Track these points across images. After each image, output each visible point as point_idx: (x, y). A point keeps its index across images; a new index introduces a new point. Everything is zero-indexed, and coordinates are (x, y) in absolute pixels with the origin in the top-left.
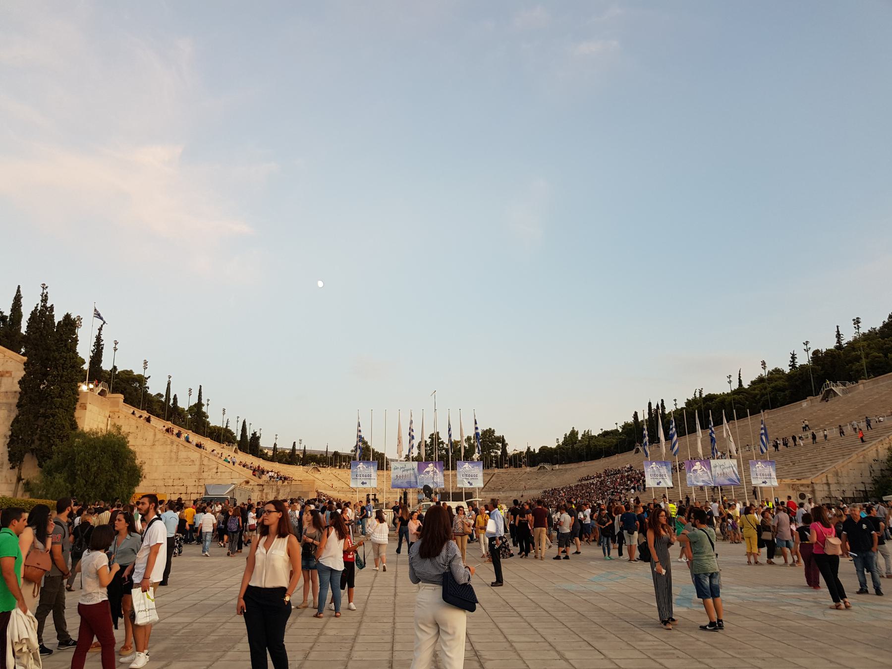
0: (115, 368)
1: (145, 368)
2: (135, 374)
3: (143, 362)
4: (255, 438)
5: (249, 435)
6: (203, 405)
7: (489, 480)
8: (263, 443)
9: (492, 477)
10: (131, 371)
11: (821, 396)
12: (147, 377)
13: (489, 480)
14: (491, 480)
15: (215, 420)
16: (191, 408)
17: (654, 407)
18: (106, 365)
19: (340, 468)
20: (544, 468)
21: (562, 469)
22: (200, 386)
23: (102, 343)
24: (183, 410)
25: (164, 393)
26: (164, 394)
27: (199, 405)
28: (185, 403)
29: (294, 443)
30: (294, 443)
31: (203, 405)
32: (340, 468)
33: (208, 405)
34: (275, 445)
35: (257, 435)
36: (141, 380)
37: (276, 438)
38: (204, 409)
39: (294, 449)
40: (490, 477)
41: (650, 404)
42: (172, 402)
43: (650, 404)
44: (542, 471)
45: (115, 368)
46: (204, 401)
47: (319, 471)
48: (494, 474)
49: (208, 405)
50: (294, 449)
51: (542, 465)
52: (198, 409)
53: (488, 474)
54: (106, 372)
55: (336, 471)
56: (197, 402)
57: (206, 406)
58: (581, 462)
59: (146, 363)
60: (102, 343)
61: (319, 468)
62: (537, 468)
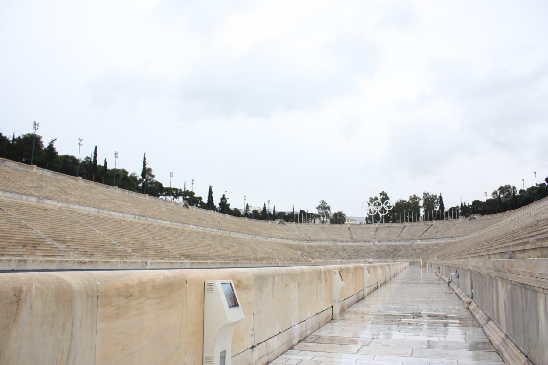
7: (426, 230)
9: (430, 227)
13: (426, 230)
14: (428, 230)
20: (474, 218)
21: (489, 219)
29: (265, 203)
30: (265, 203)
34: (247, 206)
37: (245, 199)
39: (265, 208)
40: (428, 227)
44: (473, 220)
47: (285, 224)
48: (432, 225)
50: (265, 208)
51: (472, 215)
53: (428, 225)
58: (506, 211)
61: (285, 223)
62: (469, 218)
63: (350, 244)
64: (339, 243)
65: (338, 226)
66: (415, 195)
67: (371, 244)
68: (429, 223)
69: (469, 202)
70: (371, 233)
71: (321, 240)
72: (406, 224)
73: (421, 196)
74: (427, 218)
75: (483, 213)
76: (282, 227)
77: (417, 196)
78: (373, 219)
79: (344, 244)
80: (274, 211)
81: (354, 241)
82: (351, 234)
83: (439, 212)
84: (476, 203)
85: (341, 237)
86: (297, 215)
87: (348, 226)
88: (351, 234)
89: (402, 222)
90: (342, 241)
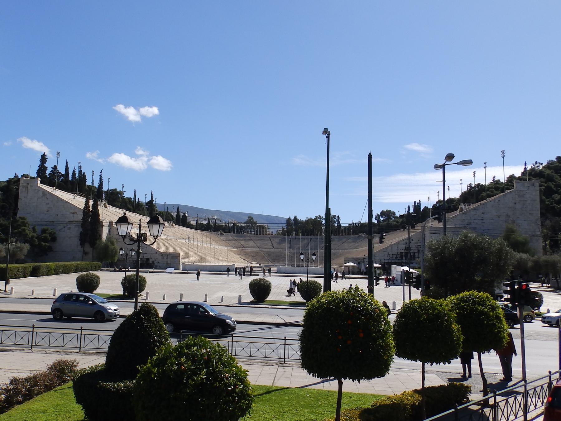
0: (109, 189)
2: (118, 190)
4: (185, 217)
6: (154, 201)
10: (116, 189)
12: (124, 191)
17: (416, 204)
18: (105, 189)
19: (237, 233)
22: (152, 191)
23: (102, 179)
25: (133, 197)
27: (152, 201)
31: (154, 201)
32: (237, 233)
33: (156, 201)
36: (121, 193)
41: (415, 201)
43: (415, 201)
45: (109, 189)
49: (156, 201)
56: (150, 199)
60: (102, 179)
82: (272, 243)
85: (265, 245)
88: (272, 243)
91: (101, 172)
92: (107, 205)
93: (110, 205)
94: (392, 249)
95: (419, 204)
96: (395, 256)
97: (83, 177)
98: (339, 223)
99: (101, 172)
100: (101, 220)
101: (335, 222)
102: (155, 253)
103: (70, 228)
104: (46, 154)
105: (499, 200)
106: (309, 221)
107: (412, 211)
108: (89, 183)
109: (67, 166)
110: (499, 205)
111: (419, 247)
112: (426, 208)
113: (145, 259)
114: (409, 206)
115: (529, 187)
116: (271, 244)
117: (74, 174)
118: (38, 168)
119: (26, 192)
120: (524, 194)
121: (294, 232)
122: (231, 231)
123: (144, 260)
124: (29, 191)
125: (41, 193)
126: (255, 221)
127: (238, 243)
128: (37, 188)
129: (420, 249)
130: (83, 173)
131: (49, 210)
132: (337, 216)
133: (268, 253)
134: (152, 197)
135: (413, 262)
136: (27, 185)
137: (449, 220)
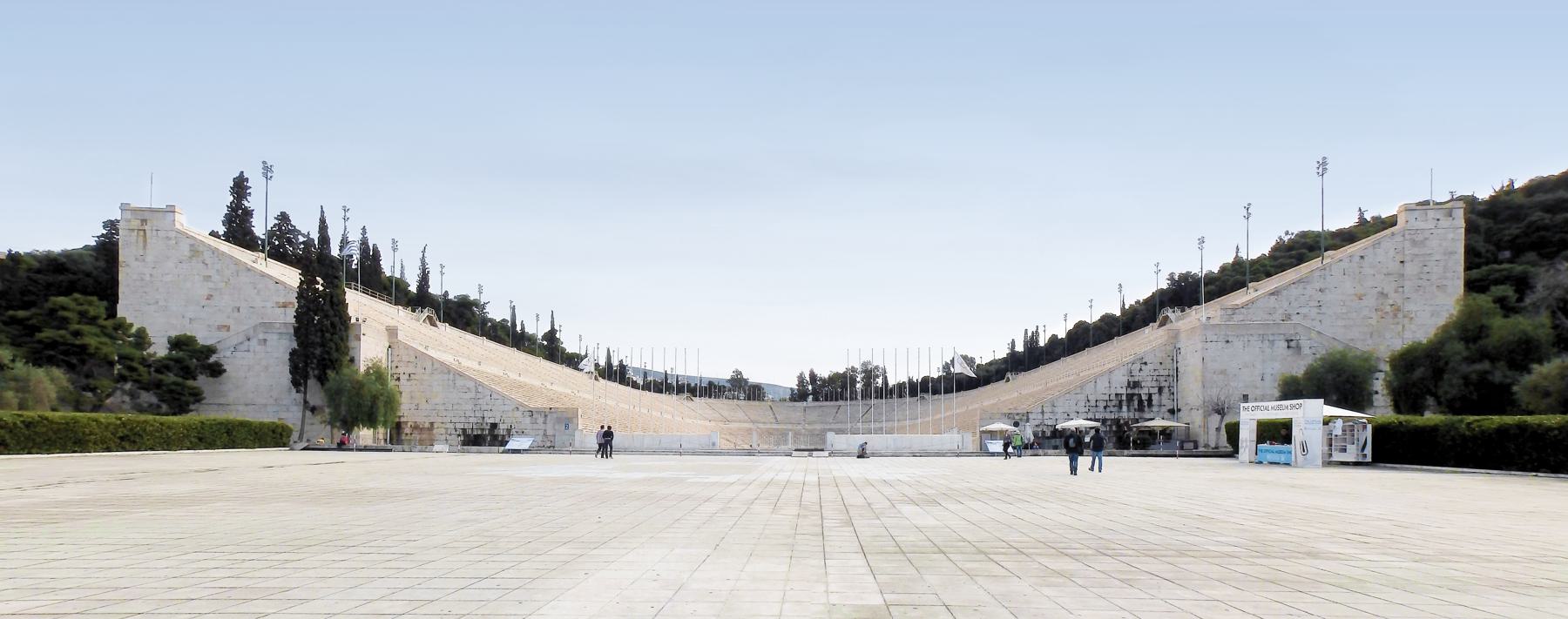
1: (481, 293)
2: (472, 299)
3: (477, 287)
4: (623, 367)
5: (615, 363)
8: (630, 374)
11: (1158, 323)
15: (570, 345)
16: (545, 337)
17: (1030, 334)
24: (533, 335)
26: (509, 320)
28: (538, 329)
35: (624, 363)
38: (558, 336)
42: (519, 328)
46: (557, 327)
52: (551, 336)
54: (435, 296)
55: (712, 401)
57: (558, 333)
59: (480, 287)
61: (693, 398)
63: (775, 426)
64: (761, 426)
65: (757, 403)
66: (852, 367)
67: (799, 427)
68: (868, 402)
69: (917, 377)
70: (798, 414)
71: (740, 421)
72: (840, 403)
73: (858, 366)
74: (866, 394)
75: (936, 392)
76: (690, 404)
77: (856, 367)
78: (799, 395)
79: (768, 426)
80: (677, 381)
81: (777, 422)
83: (882, 388)
84: (925, 380)
86: (705, 387)
87: (770, 403)
89: (836, 400)
90: (764, 423)
91: (424, 252)
92: (438, 323)
93: (447, 324)
94: (1095, 386)
95: (1036, 334)
96: (1102, 404)
97: (371, 258)
98: (885, 379)
99: (424, 252)
100: (353, 321)
101: (878, 376)
102: (513, 410)
103: (265, 340)
104: (246, 176)
105: (1362, 257)
106: (834, 378)
107: (1020, 348)
108: (387, 267)
109: (323, 222)
110: (1361, 267)
111: (1162, 379)
112: (1054, 339)
113: (487, 424)
114: (1013, 341)
115: (1438, 220)
116: (771, 415)
117: (344, 243)
118: (225, 211)
119: (141, 245)
120: (1426, 239)
121: (811, 397)
122: (706, 394)
123: (484, 426)
124: (148, 241)
125: (185, 249)
126: (745, 377)
127: (717, 415)
128: (173, 234)
129: (1163, 384)
130: (371, 248)
131: (211, 296)
132: (881, 366)
133: (767, 430)
134: (553, 325)
135: (1147, 416)
136: (142, 225)
137: (1237, 311)
